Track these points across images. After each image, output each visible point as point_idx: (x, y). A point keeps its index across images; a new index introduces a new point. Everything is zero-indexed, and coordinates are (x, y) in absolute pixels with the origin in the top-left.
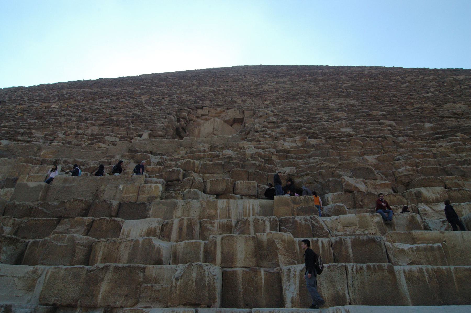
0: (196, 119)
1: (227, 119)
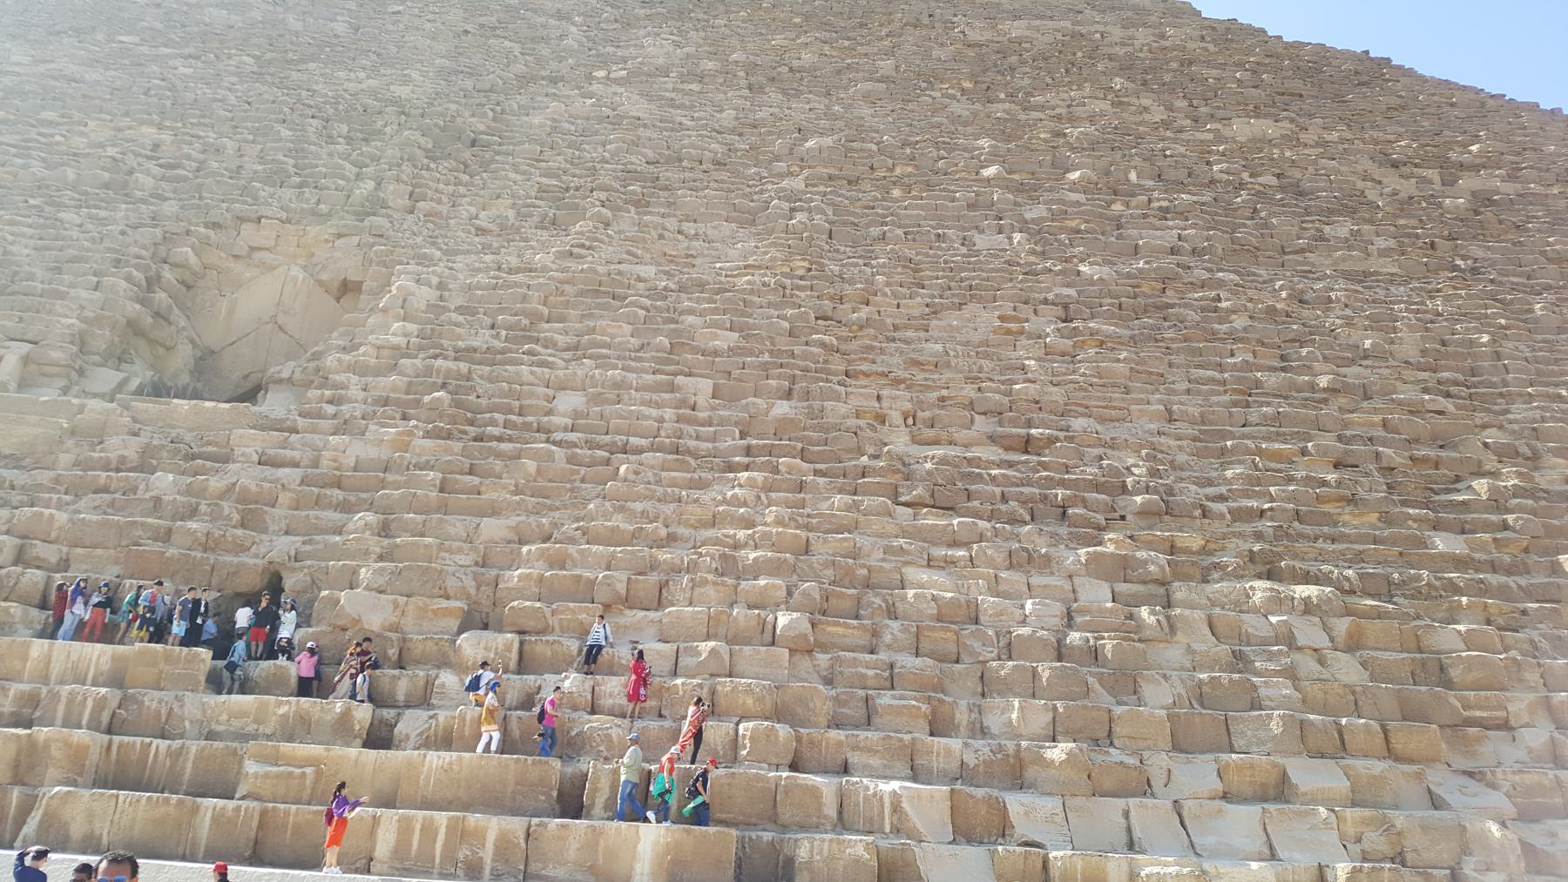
0: (231, 264)
1: (324, 277)
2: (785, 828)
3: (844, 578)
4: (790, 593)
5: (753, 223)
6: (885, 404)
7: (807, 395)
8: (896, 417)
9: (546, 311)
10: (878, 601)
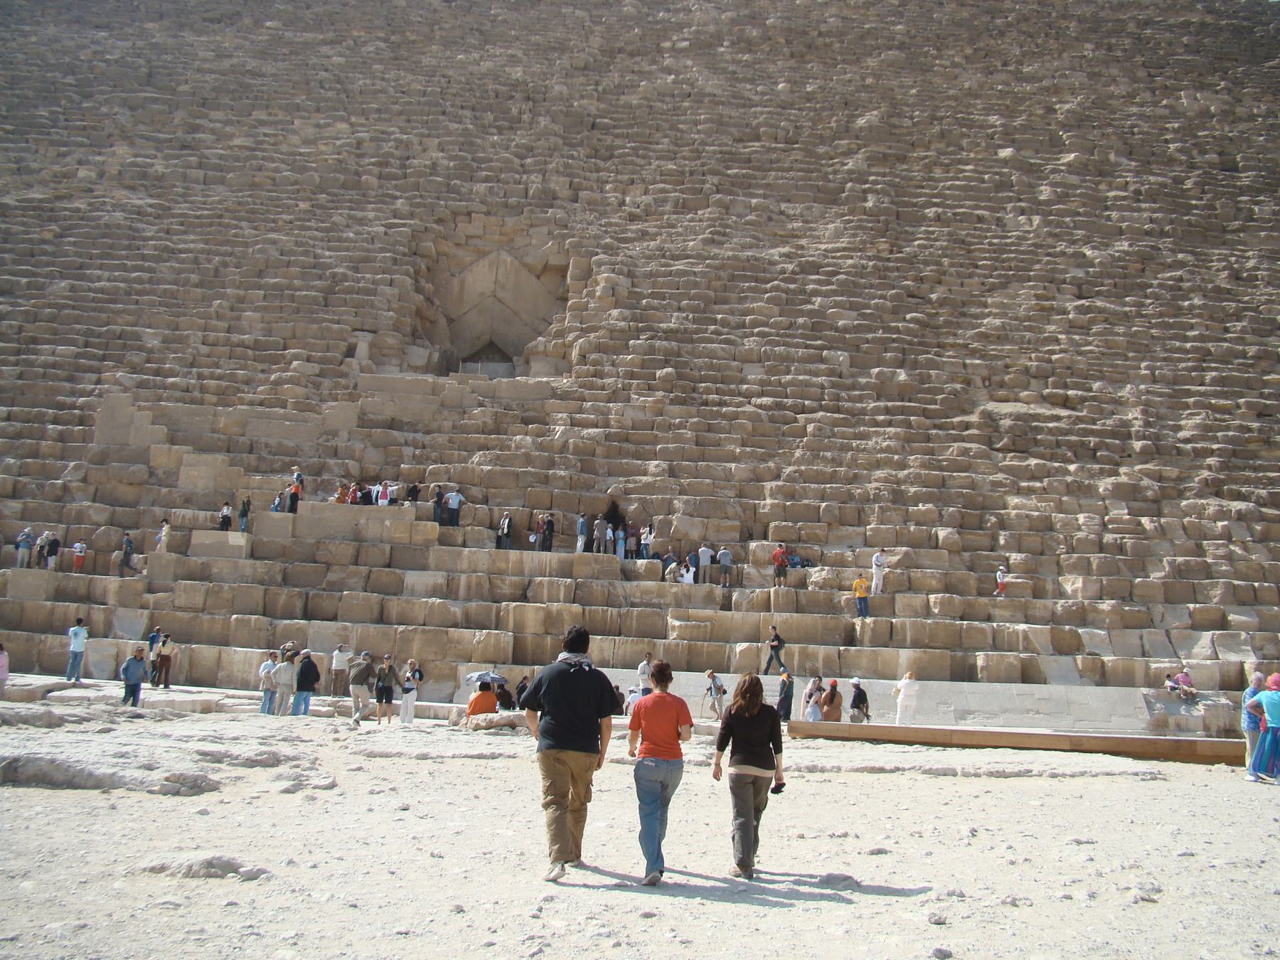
1: (529, 260)
2: (966, 650)
3: (969, 504)
4: (941, 515)
5: (835, 202)
6: (970, 371)
7: (915, 365)
9: (712, 294)
10: (993, 519)
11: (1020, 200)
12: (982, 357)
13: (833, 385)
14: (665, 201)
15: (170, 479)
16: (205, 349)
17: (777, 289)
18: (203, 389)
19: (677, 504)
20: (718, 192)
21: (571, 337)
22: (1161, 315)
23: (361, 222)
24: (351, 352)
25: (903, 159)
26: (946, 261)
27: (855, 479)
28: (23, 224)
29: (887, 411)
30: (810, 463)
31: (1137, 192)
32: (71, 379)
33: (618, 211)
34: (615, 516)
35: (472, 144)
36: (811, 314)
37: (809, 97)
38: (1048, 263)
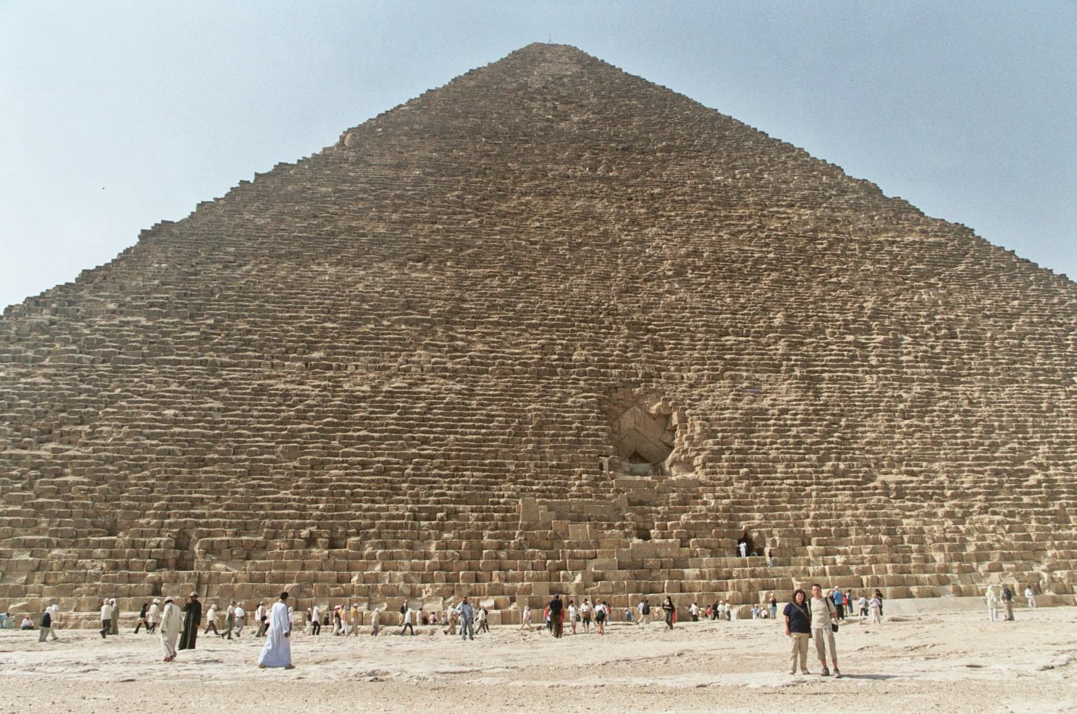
3: (889, 523)
7: (846, 460)
8: (872, 465)
11: (864, 366)
12: (874, 453)
13: (815, 472)
14: (703, 376)
15: (566, 534)
16: (539, 470)
17: (774, 425)
18: (550, 491)
19: (775, 531)
20: (726, 370)
21: (693, 453)
22: (944, 426)
23: (569, 395)
24: (601, 467)
25: (802, 344)
26: (842, 404)
27: (839, 516)
28: (407, 402)
29: (842, 483)
30: (819, 509)
31: (916, 357)
32: (487, 489)
33: (682, 383)
34: (746, 538)
35: (597, 345)
36: (795, 437)
37: (743, 307)
38: (888, 402)
